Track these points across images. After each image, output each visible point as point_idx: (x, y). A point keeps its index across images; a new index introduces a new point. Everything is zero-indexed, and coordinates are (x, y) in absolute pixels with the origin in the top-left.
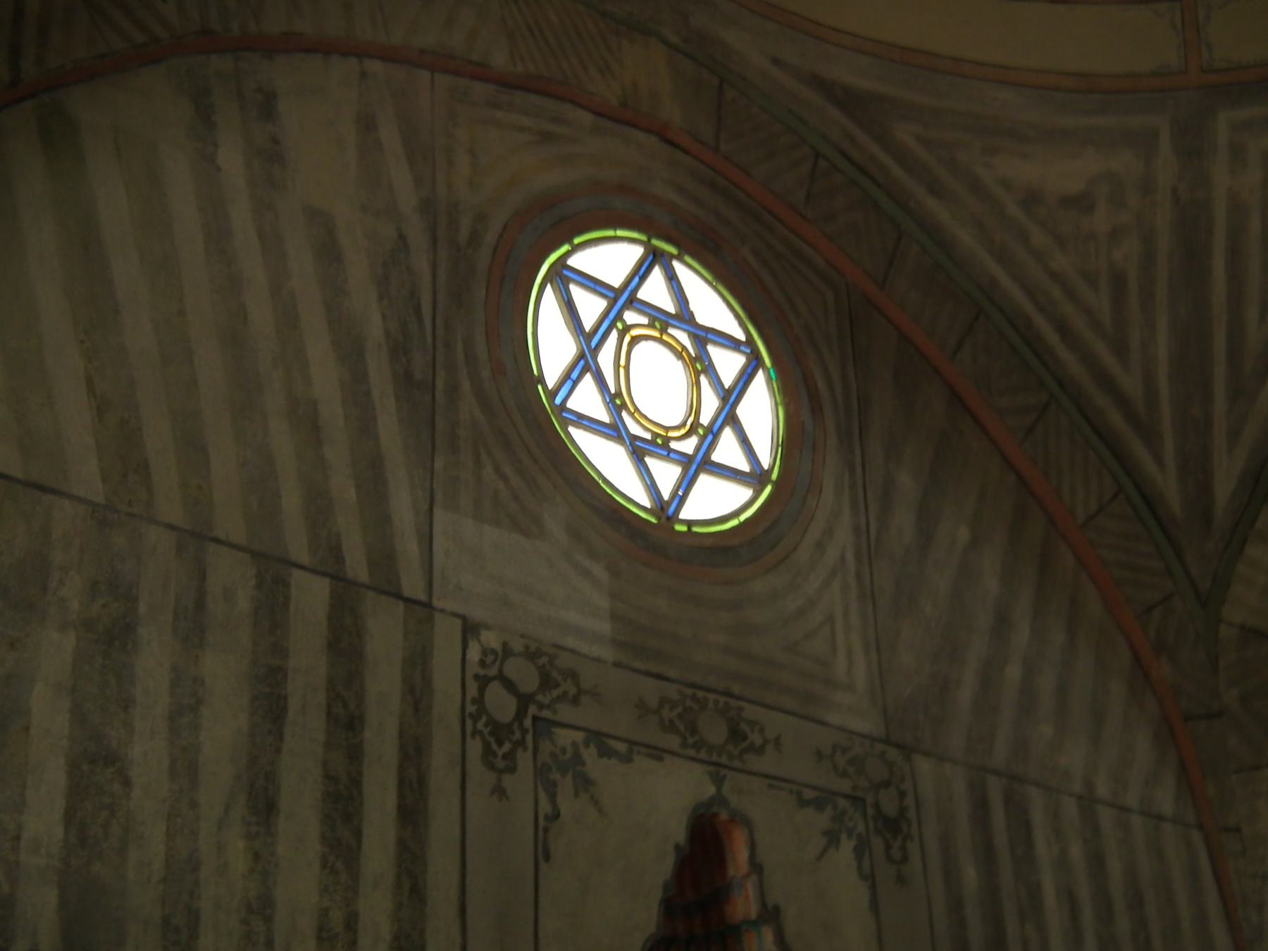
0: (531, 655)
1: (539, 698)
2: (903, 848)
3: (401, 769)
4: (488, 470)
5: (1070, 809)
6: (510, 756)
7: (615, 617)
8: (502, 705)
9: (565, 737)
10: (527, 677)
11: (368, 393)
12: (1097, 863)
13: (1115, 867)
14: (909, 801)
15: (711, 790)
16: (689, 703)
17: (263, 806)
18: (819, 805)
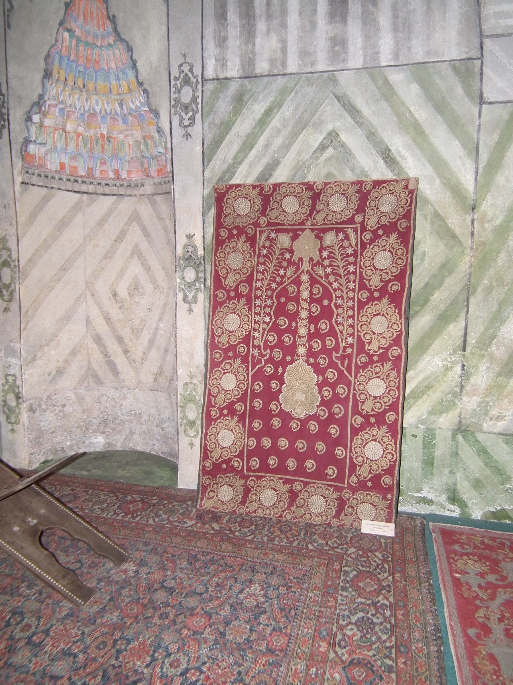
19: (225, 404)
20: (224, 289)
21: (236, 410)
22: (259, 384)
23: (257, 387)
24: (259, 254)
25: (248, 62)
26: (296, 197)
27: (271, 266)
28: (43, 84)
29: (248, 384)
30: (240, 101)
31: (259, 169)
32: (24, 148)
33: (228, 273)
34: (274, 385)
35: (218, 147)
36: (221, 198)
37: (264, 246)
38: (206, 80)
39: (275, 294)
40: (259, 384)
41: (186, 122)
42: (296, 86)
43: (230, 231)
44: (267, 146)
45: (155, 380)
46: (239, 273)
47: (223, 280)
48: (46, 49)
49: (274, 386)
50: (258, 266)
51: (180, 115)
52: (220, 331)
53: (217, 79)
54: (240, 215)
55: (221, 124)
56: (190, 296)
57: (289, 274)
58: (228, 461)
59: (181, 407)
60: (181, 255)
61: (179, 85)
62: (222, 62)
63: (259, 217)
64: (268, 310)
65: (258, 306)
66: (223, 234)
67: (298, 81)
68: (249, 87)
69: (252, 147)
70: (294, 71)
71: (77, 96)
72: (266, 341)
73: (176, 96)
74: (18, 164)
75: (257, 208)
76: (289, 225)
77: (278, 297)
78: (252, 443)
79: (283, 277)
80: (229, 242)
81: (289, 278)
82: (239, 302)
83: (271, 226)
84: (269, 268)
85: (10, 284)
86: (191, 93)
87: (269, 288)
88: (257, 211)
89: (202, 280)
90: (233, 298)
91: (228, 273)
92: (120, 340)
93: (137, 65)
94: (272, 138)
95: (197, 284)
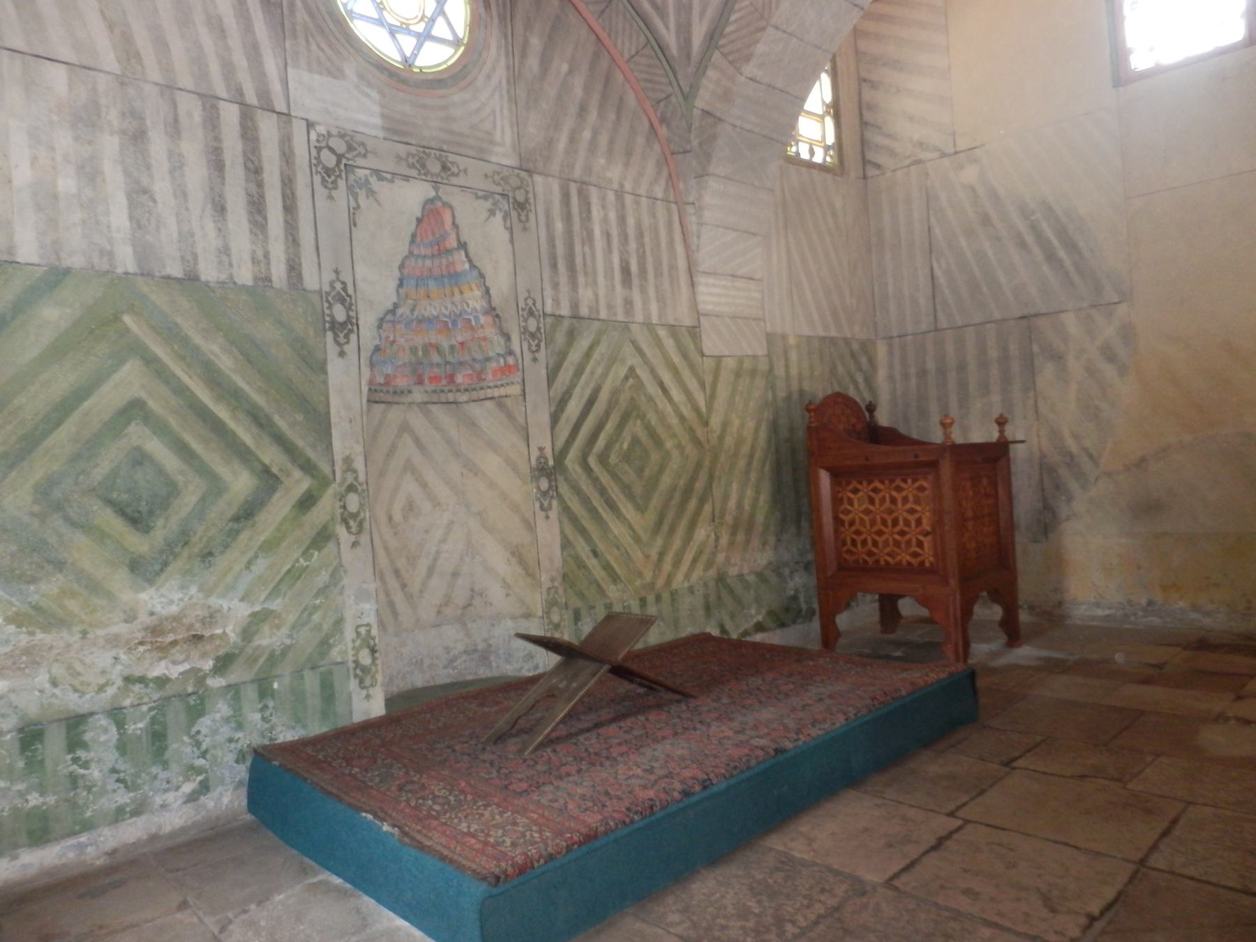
0: (342, 136)
2: (527, 216)
4: (314, 47)
5: (611, 196)
7: (383, 116)
8: (329, 159)
9: (361, 173)
10: (340, 147)
11: (247, 10)
12: (622, 220)
13: (631, 221)
14: (531, 196)
15: (433, 194)
17: (220, 209)
18: (485, 198)
25: (575, 306)
30: (572, 335)
41: (534, 348)
44: (592, 373)
45: (439, 612)
48: (400, 258)
56: (546, 504)
85: (358, 512)
92: (397, 573)
93: (492, 292)
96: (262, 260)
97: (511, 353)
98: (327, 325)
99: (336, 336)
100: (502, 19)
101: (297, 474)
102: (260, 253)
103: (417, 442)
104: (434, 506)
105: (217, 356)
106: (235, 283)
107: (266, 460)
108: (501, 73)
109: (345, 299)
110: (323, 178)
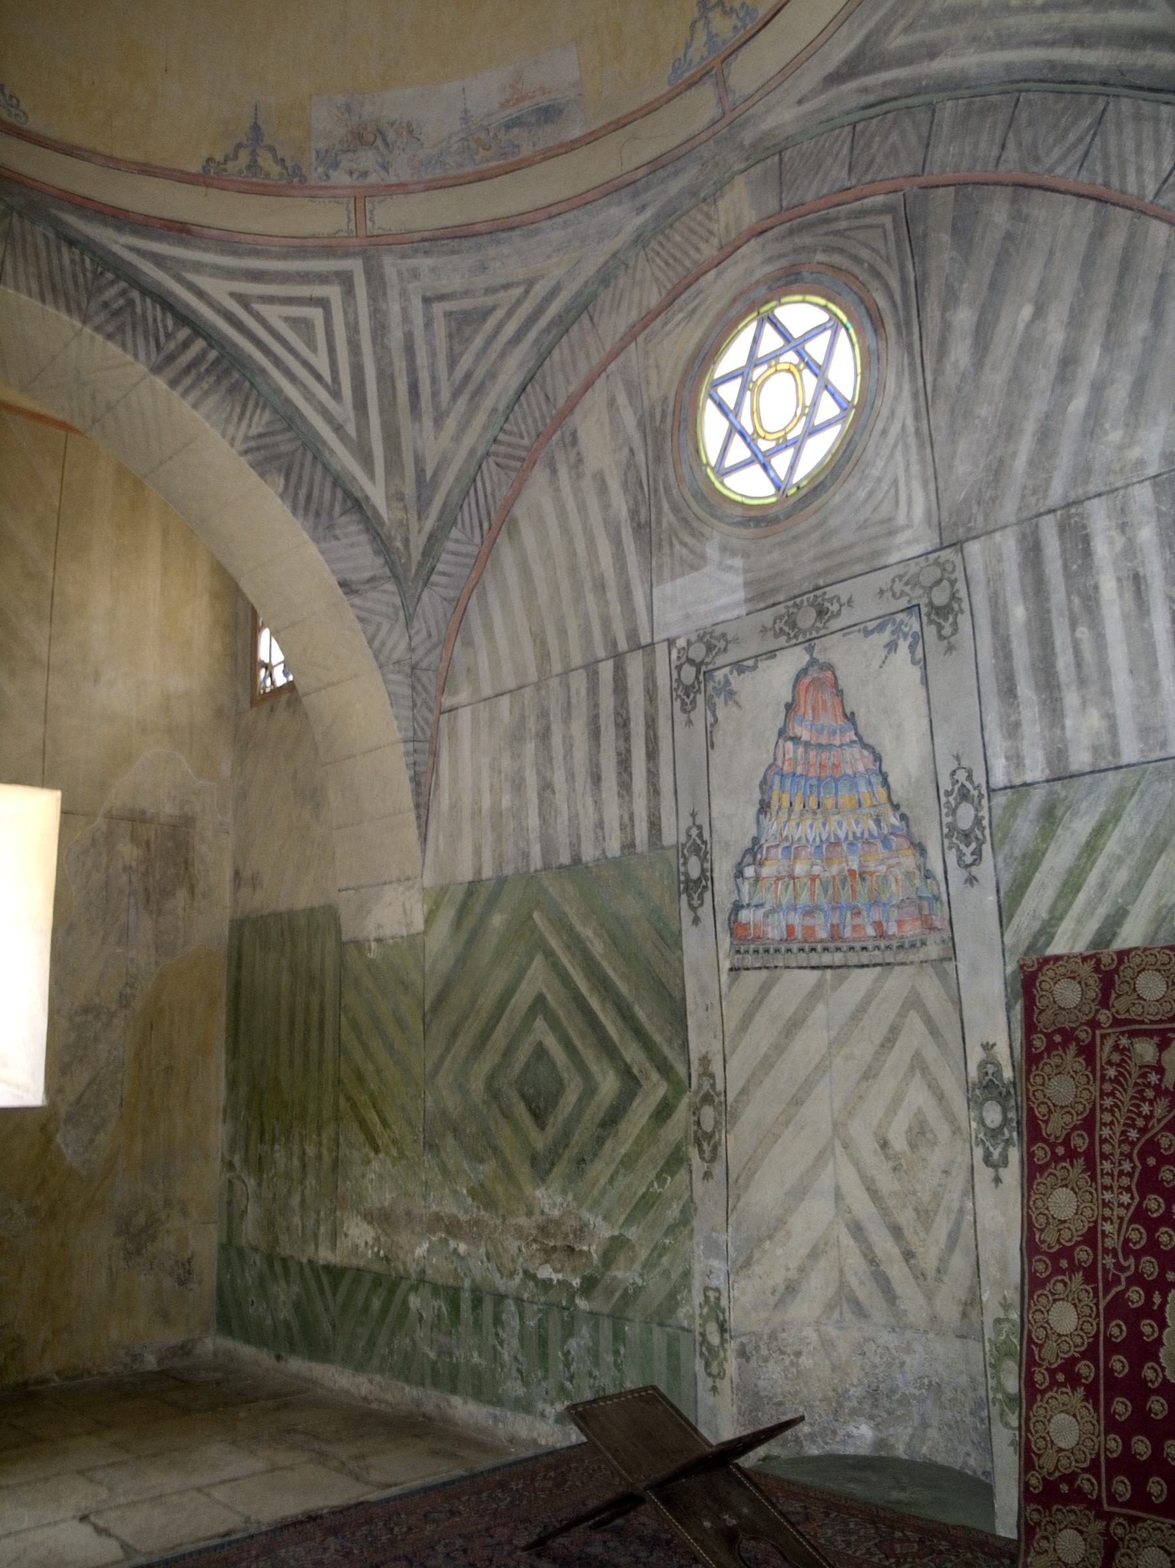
1: (707, 660)
2: (955, 623)
3: (647, 734)
4: (677, 546)
6: (694, 701)
9: (719, 675)
10: (698, 652)
14: (961, 585)
15: (808, 657)
16: (791, 610)
18: (880, 628)
19: (1060, 1362)
20: (1045, 1141)
21: (1079, 1375)
22: (1119, 1326)
23: (1115, 1331)
24: (1103, 1076)
25: (1058, 754)
26: (1159, 970)
27: (1126, 1098)
28: (758, 822)
29: (1098, 1324)
30: (1050, 818)
31: (1093, 926)
32: (733, 917)
33: (1050, 1112)
34: (1147, 1327)
35: (1022, 895)
36: (1028, 983)
37: (1110, 1063)
38: (994, 790)
39: (1136, 1151)
40: (1119, 1326)
41: (969, 859)
42: (1139, 783)
43: (1049, 1037)
44: (1103, 886)
46: (1069, 1113)
47: (1043, 1126)
48: (762, 771)
49: (1146, 1330)
50: (1102, 1098)
51: (958, 849)
52: (1042, 1219)
53: (1012, 787)
54: (1064, 1009)
55: (1024, 856)
56: (996, 1154)
57: (1158, 1112)
58: (1070, 1478)
59: (993, 1366)
60: (976, 1080)
61: (953, 803)
62: (1016, 760)
63: (1097, 1011)
64: (1125, 1181)
65: (1108, 1174)
66: (1037, 1043)
67: (1145, 772)
68: (1063, 794)
69: (1078, 890)
70: (1133, 760)
71: (808, 822)
72: (1127, 1241)
73: (950, 819)
74: (725, 941)
75: (1092, 995)
76: (1152, 1022)
77: (1142, 1156)
78: (1115, 1444)
79: (1147, 1118)
80: (1049, 1057)
81: (1159, 1121)
82: (1072, 1165)
83: (1121, 1026)
84: (1122, 1103)
86: (973, 813)
87: (1125, 1139)
88: (1093, 1001)
89: (1014, 1124)
90: (1062, 1159)
91: (1050, 1112)
93: (890, 779)
94: (1111, 871)
95: (1006, 1131)
96: (627, 825)
97: (928, 875)
98: (682, 886)
99: (690, 897)
100: (903, 328)
101: (655, 1076)
102: (626, 817)
103: (929, 1021)
104: (954, 1133)
105: (592, 943)
106: (606, 858)
107: (628, 1060)
108: (905, 410)
109: (699, 847)
110: (683, 700)
